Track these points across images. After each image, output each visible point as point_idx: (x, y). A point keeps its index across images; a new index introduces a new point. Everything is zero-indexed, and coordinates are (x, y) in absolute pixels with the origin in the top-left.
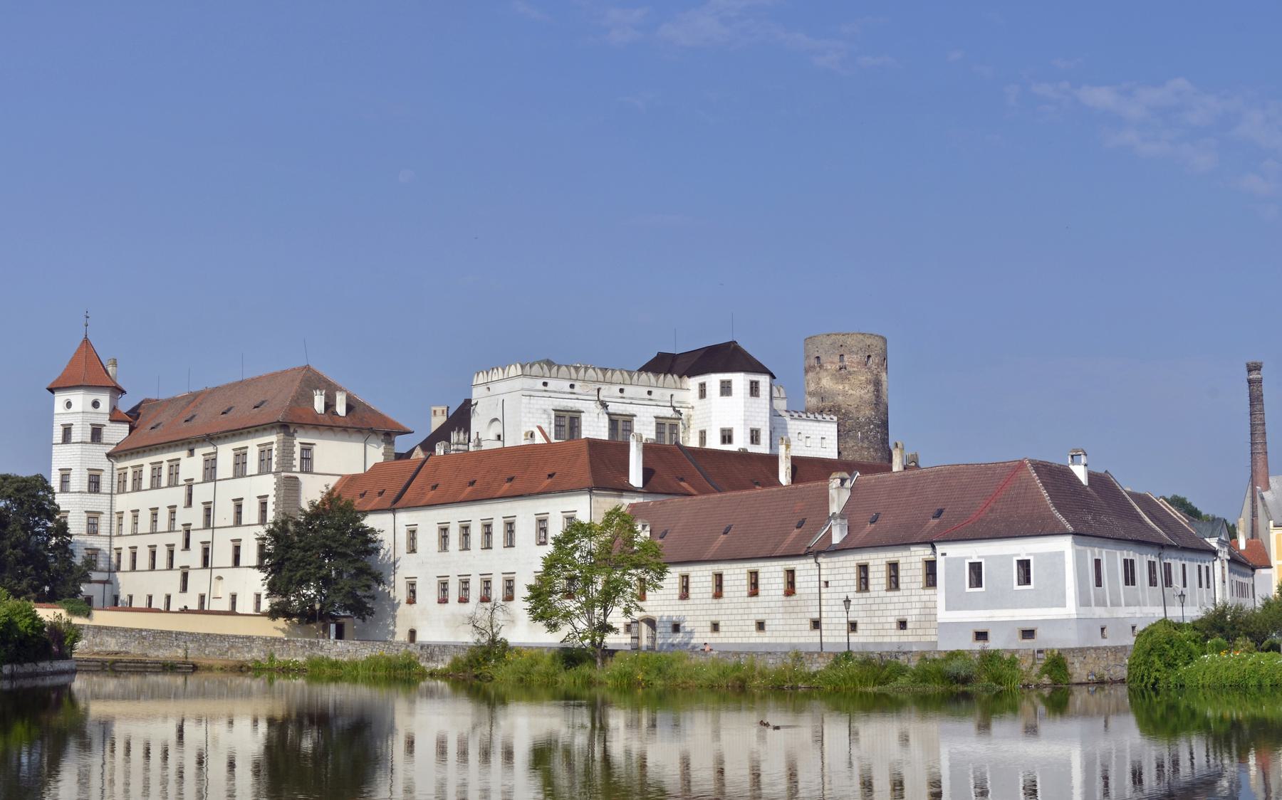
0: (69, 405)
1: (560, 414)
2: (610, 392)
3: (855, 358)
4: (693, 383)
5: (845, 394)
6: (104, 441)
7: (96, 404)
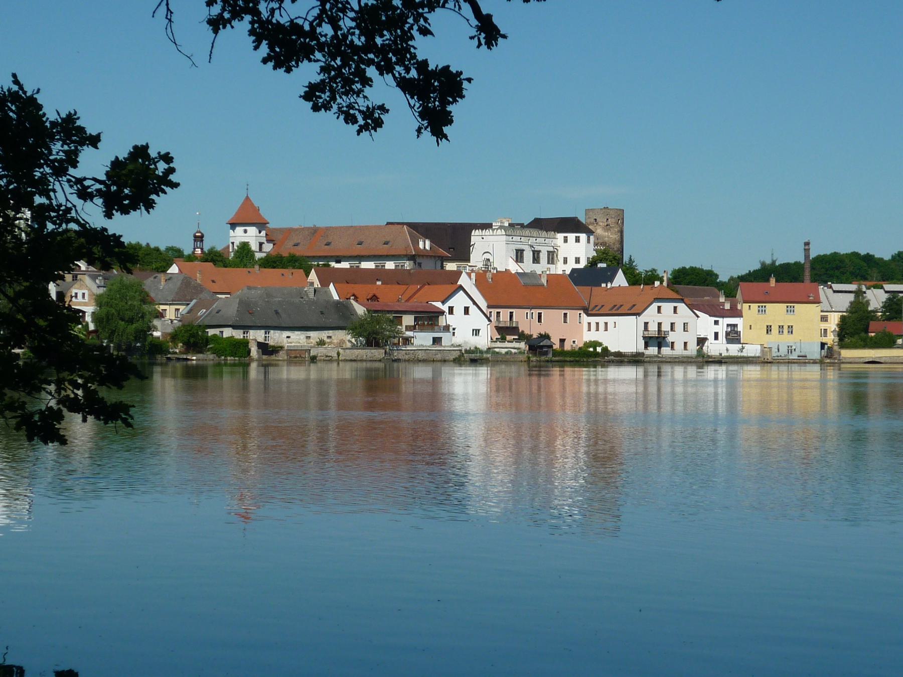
0: (245, 231)
1: (517, 251)
2: (532, 240)
3: (613, 220)
4: (560, 236)
5: (608, 237)
6: (264, 250)
7: (260, 232)
